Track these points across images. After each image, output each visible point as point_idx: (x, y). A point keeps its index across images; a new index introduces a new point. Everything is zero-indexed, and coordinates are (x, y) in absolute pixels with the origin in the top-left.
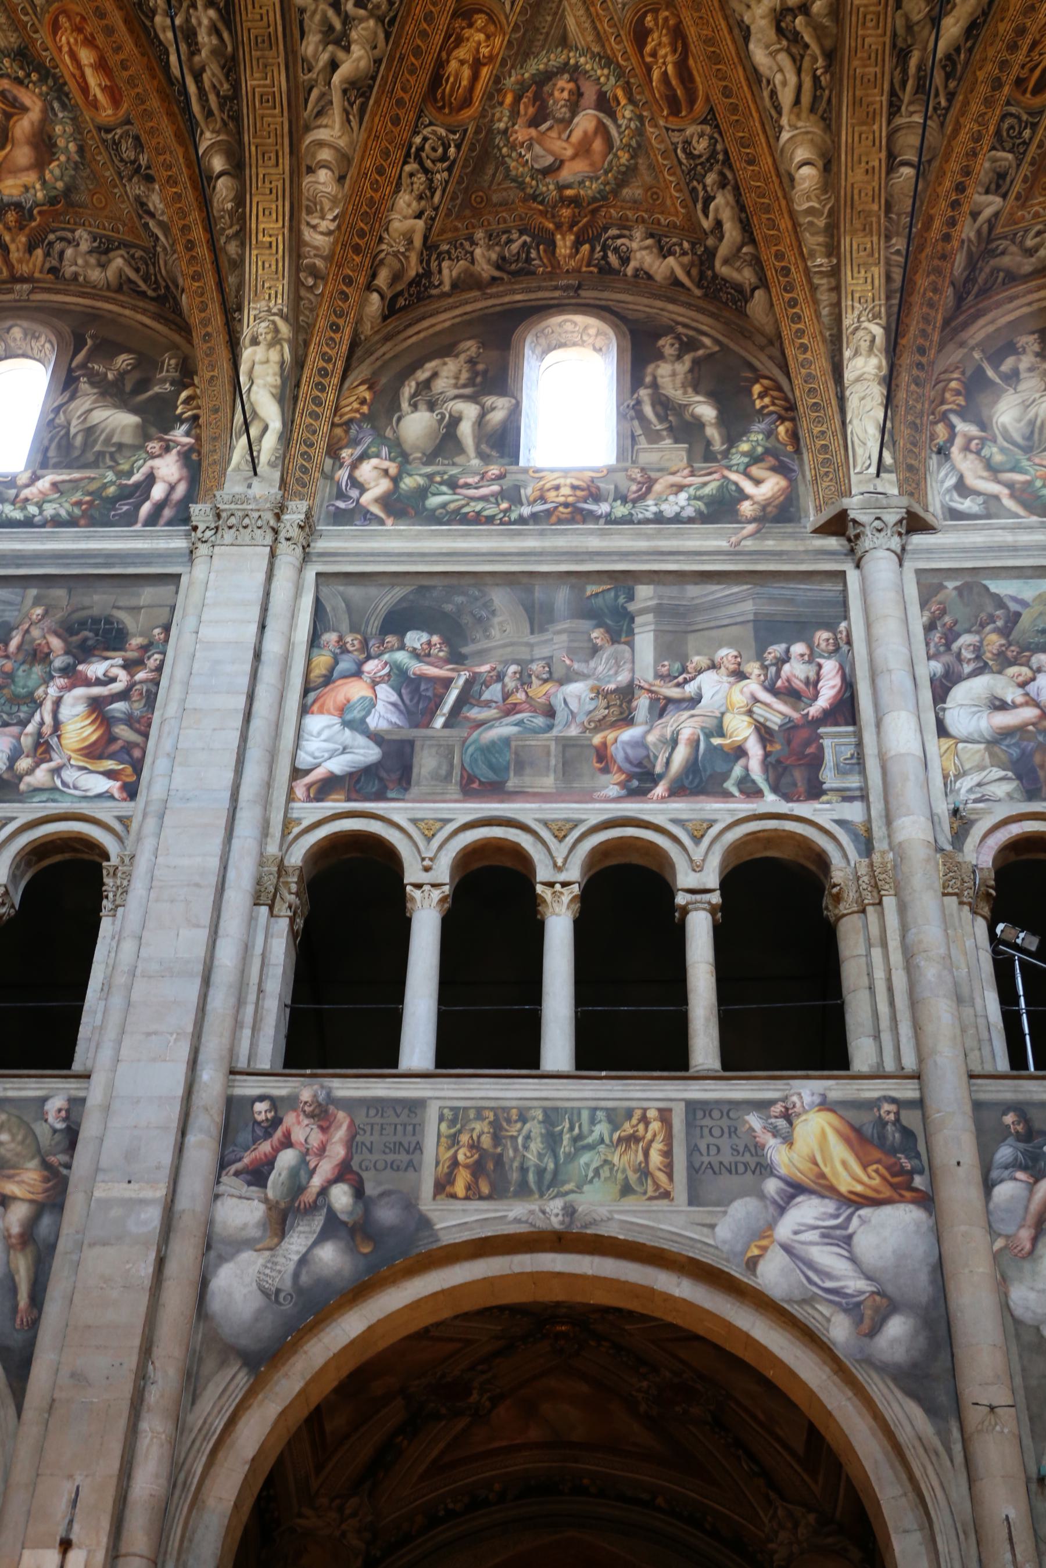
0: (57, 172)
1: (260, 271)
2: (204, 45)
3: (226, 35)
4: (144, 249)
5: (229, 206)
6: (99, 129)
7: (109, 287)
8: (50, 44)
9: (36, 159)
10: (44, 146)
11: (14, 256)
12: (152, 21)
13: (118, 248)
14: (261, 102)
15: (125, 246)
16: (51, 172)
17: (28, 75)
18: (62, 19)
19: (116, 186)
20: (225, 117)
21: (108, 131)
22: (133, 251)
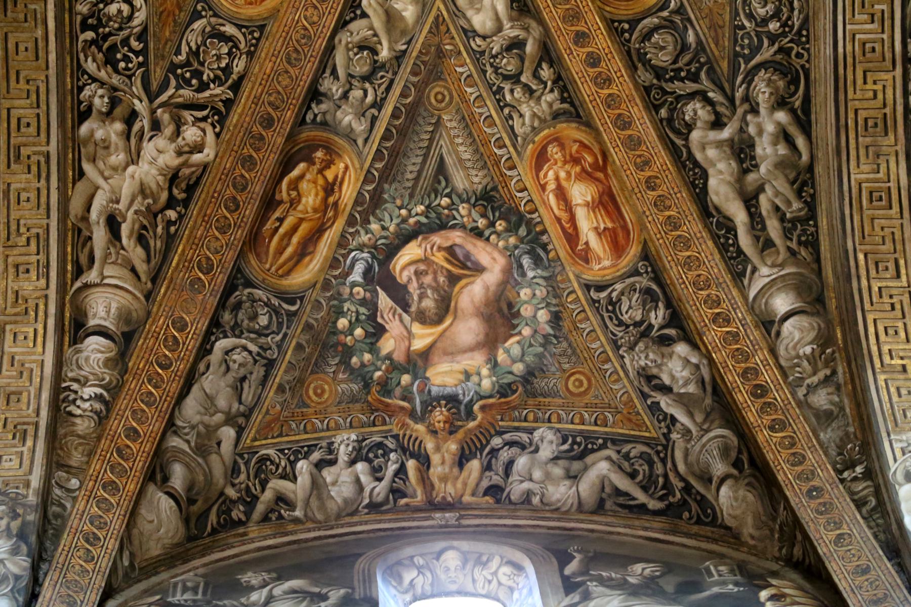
0: (516, 350)
1: (895, 398)
2: (765, 158)
3: (801, 142)
4: (647, 442)
5: (808, 350)
6: (587, 287)
7: (580, 507)
8: (529, 182)
9: (487, 335)
10: (501, 316)
11: (437, 470)
12: (687, 139)
13: (603, 447)
14: (871, 201)
15: (614, 442)
16: (507, 351)
17: (492, 224)
18: (553, 150)
19: (608, 360)
20: (794, 245)
21: (600, 288)
22: (626, 448)
